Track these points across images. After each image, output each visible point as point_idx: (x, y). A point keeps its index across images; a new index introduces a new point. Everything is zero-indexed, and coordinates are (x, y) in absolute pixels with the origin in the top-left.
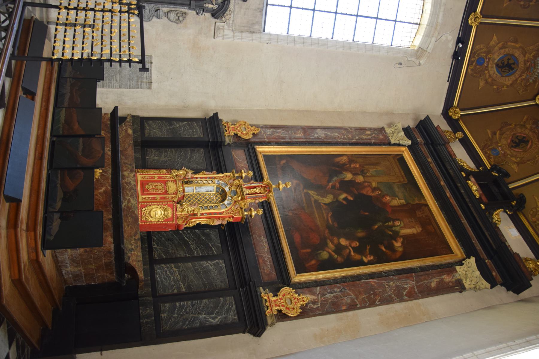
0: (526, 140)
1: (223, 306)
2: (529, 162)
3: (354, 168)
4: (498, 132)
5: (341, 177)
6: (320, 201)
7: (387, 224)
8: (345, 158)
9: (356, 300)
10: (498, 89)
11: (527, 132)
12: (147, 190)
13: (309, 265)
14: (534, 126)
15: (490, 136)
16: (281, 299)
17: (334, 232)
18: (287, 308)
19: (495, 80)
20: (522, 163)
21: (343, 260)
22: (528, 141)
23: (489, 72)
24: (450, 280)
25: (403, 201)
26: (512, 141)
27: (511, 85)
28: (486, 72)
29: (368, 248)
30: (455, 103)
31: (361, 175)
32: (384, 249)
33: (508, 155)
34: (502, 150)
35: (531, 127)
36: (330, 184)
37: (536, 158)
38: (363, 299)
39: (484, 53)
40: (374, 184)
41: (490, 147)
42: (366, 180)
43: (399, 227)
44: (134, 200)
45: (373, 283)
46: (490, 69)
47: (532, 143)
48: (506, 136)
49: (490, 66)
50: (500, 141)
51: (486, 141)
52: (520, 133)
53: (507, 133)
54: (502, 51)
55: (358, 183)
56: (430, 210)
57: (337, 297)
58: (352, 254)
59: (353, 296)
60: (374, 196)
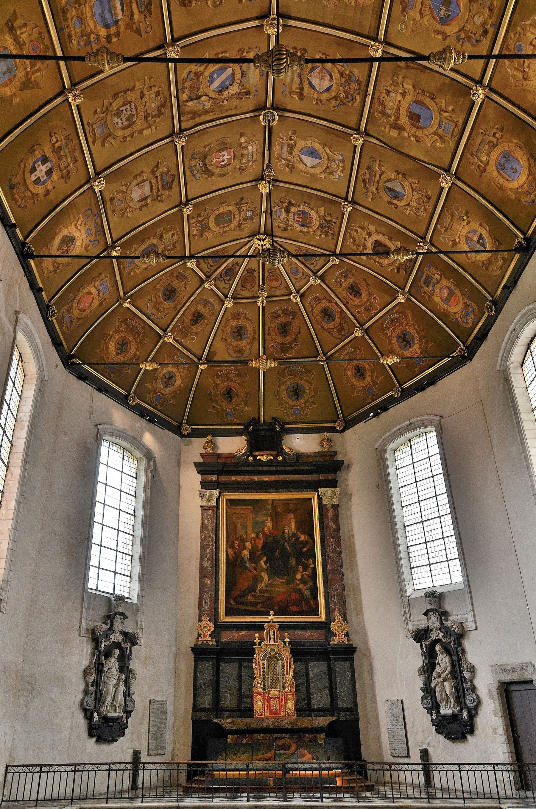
0: (228, 390)
3: (238, 545)
5: (246, 558)
7: (287, 539)
8: (229, 550)
14: (220, 379)
18: (344, 629)
25: (269, 518)
27: (182, 380)
28: (166, 396)
29: (303, 560)
32: (305, 549)
35: (220, 381)
36: (252, 570)
40: (253, 535)
47: (233, 387)
53: (217, 398)
54: (158, 381)
57: (338, 596)
58: (307, 573)
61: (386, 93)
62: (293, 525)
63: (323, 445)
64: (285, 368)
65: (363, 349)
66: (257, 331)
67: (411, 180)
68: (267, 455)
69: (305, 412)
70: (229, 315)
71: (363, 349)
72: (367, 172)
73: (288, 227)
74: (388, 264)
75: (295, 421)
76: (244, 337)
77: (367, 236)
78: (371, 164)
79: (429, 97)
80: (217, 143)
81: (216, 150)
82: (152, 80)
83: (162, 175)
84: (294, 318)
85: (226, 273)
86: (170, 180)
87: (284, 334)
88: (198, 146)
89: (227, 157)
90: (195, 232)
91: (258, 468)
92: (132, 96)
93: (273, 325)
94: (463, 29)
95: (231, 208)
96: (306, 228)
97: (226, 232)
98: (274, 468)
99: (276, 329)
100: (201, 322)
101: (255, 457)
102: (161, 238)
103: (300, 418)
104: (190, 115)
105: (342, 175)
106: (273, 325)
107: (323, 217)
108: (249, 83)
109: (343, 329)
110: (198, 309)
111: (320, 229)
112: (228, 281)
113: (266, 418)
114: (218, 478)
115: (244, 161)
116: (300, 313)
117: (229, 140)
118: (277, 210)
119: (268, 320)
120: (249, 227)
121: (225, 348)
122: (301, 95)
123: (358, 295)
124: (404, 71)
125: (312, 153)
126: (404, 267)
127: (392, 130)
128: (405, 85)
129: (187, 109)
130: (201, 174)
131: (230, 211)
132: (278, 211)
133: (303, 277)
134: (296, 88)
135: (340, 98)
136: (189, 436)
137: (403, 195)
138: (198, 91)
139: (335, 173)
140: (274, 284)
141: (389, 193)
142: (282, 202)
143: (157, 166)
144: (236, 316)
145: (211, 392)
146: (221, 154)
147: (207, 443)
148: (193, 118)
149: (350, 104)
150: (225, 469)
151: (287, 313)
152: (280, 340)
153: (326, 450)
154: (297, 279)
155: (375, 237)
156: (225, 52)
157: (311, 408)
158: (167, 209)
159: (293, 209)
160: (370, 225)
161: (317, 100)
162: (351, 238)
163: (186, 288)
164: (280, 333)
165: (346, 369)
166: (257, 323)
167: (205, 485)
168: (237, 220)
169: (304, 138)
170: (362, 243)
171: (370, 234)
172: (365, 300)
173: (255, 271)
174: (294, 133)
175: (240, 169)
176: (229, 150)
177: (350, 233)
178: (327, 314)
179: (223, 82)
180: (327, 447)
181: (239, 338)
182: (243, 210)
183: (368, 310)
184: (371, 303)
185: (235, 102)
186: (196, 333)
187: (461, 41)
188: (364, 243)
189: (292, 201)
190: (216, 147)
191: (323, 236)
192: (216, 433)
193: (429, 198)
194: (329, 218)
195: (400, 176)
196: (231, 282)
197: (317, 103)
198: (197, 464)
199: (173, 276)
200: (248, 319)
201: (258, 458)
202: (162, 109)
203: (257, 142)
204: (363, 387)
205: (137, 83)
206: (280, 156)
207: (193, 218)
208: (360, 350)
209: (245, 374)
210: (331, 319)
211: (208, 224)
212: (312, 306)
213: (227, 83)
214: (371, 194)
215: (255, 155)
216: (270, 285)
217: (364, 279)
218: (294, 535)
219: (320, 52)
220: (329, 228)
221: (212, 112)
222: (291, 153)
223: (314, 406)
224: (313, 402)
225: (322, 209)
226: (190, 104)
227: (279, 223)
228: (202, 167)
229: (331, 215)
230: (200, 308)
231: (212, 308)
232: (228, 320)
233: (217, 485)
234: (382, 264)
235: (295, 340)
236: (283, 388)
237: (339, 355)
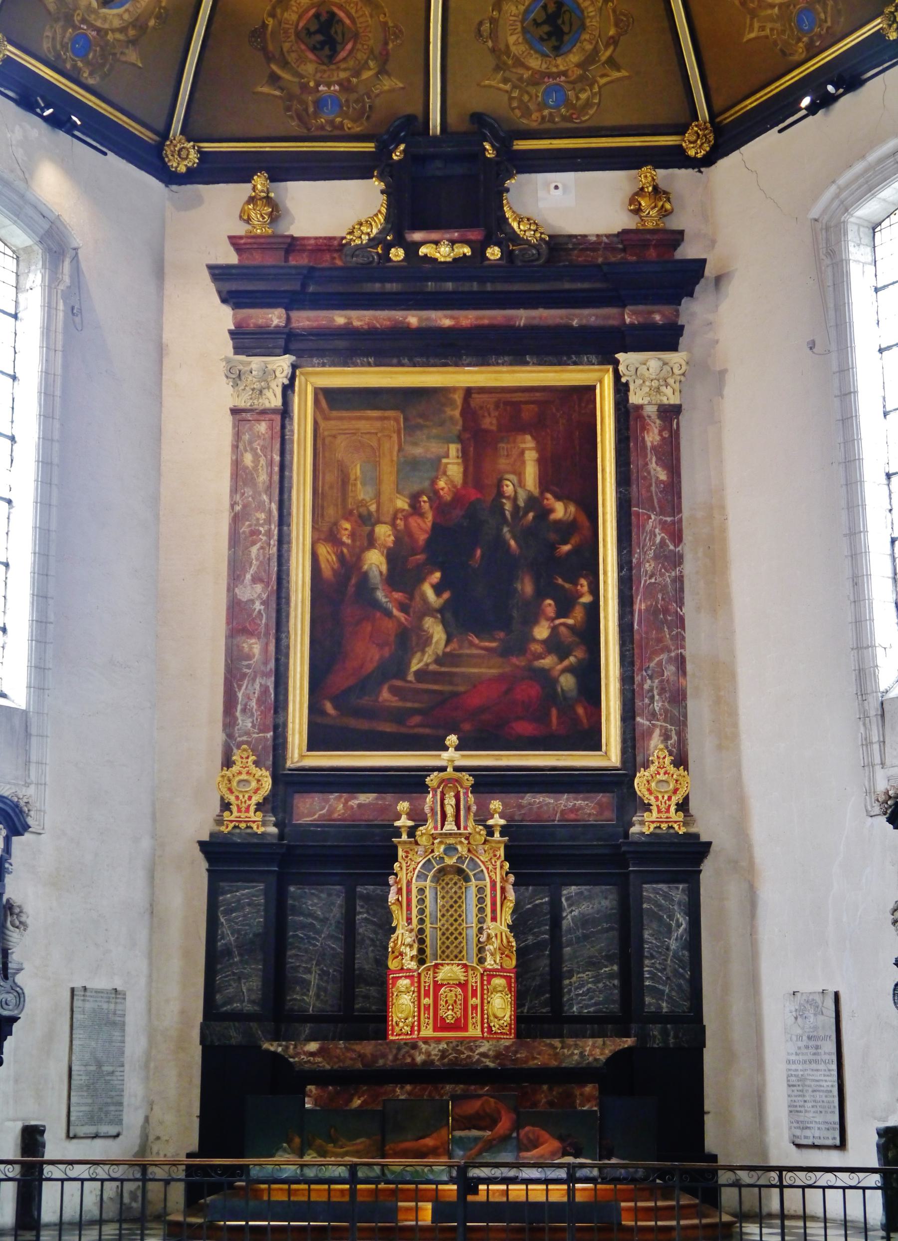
0: (324, 17)
1: (660, 906)
2: (391, 46)
4: (274, 67)
5: (375, 578)
6: (440, 652)
7: (508, 514)
9: (673, 654)
10: (158, 17)
12: (458, 1020)
13: (585, 721)
15: (277, 93)
16: (657, 798)
17: (519, 644)
18: (675, 791)
19: (137, 19)
20: (385, 62)
21: (584, 648)
22: (333, 15)
23: (113, 31)
24: (656, 431)
26: (313, 49)
28: (110, 37)
29: (560, 581)
30: (147, 136)
31: (373, 525)
33: (349, 81)
34: (328, 85)
36: (395, 612)
37: (386, 23)
38: (671, 639)
39: (64, 31)
41: (311, 109)
42: (388, 519)
43: (520, 491)
44: (480, 1046)
45: (643, 607)
46: (106, 26)
47: (341, 7)
48: (294, 55)
49: (98, 24)
50: (301, 76)
51: (288, 109)
52: (300, 17)
53: (286, 46)
55: (395, 542)
56: (482, 390)
57: (662, 691)
59: (664, 657)
60: (434, 517)
62: (531, 472)
63: (638, 211)
68: (453, 242)
69: (583, 96)
75: (547, 125)
91: (420, 284)
98: (475, 286)
101: (412, 249)
103: (564, 118)
113: (451, 119)
114: (288, 319)
136: (191, 177)
145: (264, 26)
147: (252, 200)
150: (311, 289)
153: (650, 225)
157: (602, 81)
167: (246, 340)
180: (651, 218)
192: (285, 169)
198: (218, 273)
201: (423, 251)
204: (780, 6)
218: (533, 502)
223: (616, 75)
224: (612, 62)
233: (288, 341)
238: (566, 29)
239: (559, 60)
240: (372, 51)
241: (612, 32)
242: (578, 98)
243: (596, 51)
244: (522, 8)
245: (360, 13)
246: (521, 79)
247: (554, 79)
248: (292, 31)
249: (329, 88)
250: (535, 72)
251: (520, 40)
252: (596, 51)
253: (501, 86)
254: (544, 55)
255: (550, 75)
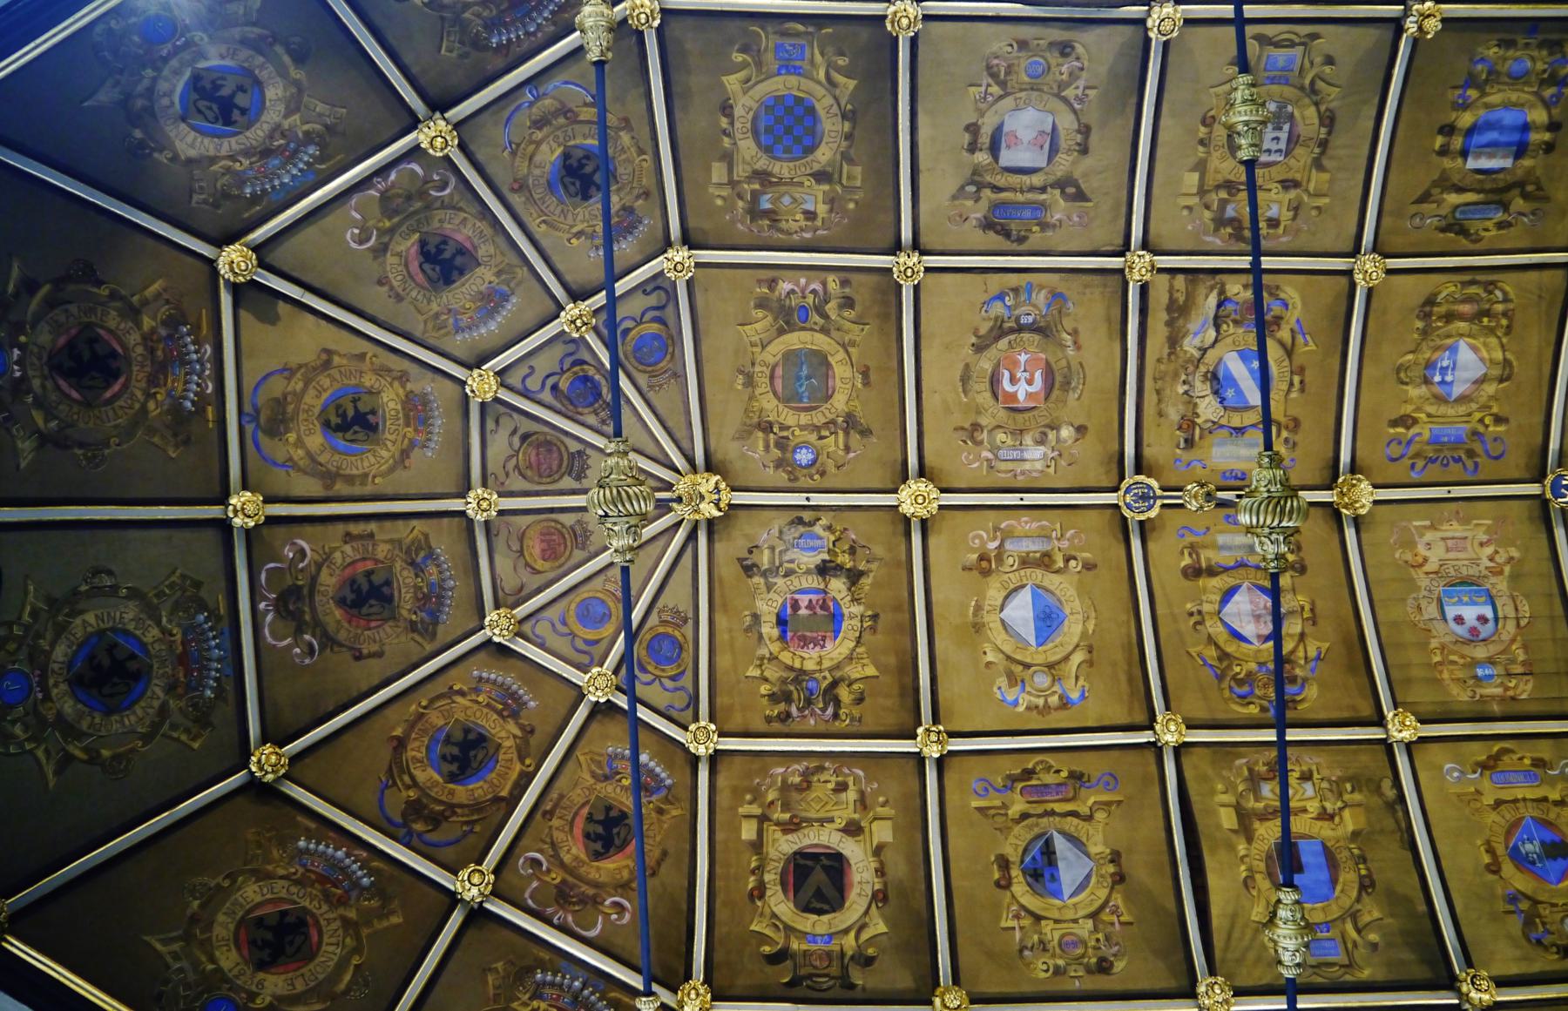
2: (79, 452)
11: (134, 338)
14: (163, 332)
22: (115, 375)
35: (153, 331)
37: (108, 445)
47: (125, 386)
52: (110, 331)
61: (1303, 773)
64: (213, 615)
65: (396, 920)
66: (357, 490)
67: (1118, 899)
69: (18, 730)
70: (424, 384)
71: (396, 920)
72: (1064, 774)
73: (764, 574)
74: (774, 915)
76: (339, 441)
77: (840, 823)
78: (1093, 781)
79: (1361, 877)
80: (1074, 364)
81: (1052, 361)
82: (1314, 213)
83: (1043, 206)
84: (413, 626)
85: (586, 379)
86: (1013, 226)
87: (350, 597)
88: (1087, 312)
89: (1022, 390)
90: (784, 286)
92: (1303, 155)
93: (382, 551)
94: (1536, 902)
95: (840, 402)
96: (776, 632)
97: (750, 381)
99: (370, 565)
100: (420, 278)
102: (821, 176)
104: (1181, 299)
105: (1021, 709)
106: (382, 551)
107: (842, 679)
108: (1212, 445)
109: (436, 821)
110: (480, 271)
111: (792, 675)
112: (554, 388)
115: (1000, 436)
116: (429, 648)
117: (1073, 396)
118: (820, 538)
119: (401, 530)
120: (755, 455)
121: (294, 361)
122: (1194, 572)
123: (598, 846)
124: (1376, 801)
125: (1048, 620)
126: (803, 972)
127: (1232, 811)
128: (1347, 813)
129: (1202, 290)
130: (996, 319)
131: (828, 397)
132: (818, 543)
133: (581, 645)
134: (1208, 560)
135: (1229, 667)
137: (1057, 894)
138: (1236, 322)
139: (1018, 688)
140: (534, 548)
141: (1036, 849)
142: (852, 551)
143: (1081, 196)
144: (417, 410)
145: (99, 283)
146: (1038, 375)
148: (1172, 306)
149: (1227, 693)
151: (431, 601)
152: (329, 580)
154: (564, 623)
155: (852, 850)
156: (1302, 390)
157: (40, 753)
158: (924, 207)
159: (838, 586)
160: (889, 823)
161: (1200, 612)
162: (807, 775)
163: (578, 235)
164: (353, 582)
165: (263, 876)
166: (389, 491)
168: (789, 418)
169: (1082, 590)
170: (804, 814)
171: (853, 829)
172: (594, 875)
173: (578, 478)
174: (1089, 566)
175: (976, 427)
176: (1042, 395)
177: (821, 769)
178: (467, 752)
179: (1233, 382)
181: (335, 420)
182: (821, 438)
183: (563, 895)
184: (596, 901)
185: (1174, 414)
186: (381, 251)
187: (1512, 908)
188: (810, 821)
189: (866, 582)
190: (1063, 363)
191: (764, 689)
193: (1103, 967)
194: (844, 694)
195: (1111, 869)
196: (547, 396)
197: (1191, 614)
199: (638, 197)
200: (405, 454)
202: (1229, 230)
203: (1052, 470)
205: (1325, 176)
206: (1007, 535)
207: (845, 283)
208: (383, 913)
209: (187, 442)
210: (454, 767)
211: (804, 329)
212: (477, 691)
213: (1230, 393)
214: (997, 803)
215: (1010, 466)
216: (531, 533)
217: (665, 854)
219: (1313, 603)
220: (809, 702)
221: (1169, 355)
222: (1025, 562)
223: (49, 771)
224: (68, 759)
225: (871, 671)
226: (1213, 300)
227: (772, 549)
228: (1018, 319)
229: (860, 700)
230: (481, 278)
231: (465, 320)
232: (403, 378)
234: (762, 896)
235: (328, 641)
236: (129, 614)
237: (308, 830)
238: (106, 690)
239: (64, 687)
240: (71, 426)
241: (106, 753)
242: (14, 722)
243: (80, 735)
244: (131, 627)
245: (120, 413)
246: (39, 636)
247: (39, 684)
248: (93, 319)
249: (16, 363)
250: (48, 654)
251: (89, 629)
252: (80, 735)
253: (28, 608)
254: (70, 665)
255: (43, 678)
